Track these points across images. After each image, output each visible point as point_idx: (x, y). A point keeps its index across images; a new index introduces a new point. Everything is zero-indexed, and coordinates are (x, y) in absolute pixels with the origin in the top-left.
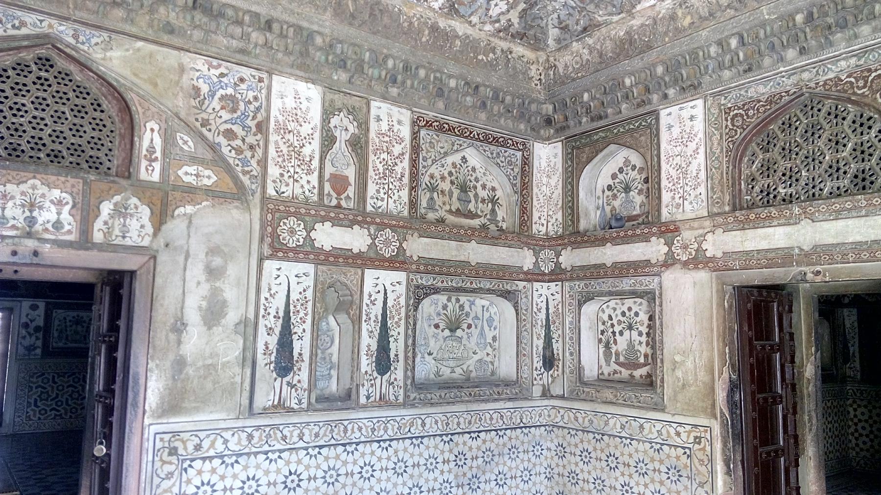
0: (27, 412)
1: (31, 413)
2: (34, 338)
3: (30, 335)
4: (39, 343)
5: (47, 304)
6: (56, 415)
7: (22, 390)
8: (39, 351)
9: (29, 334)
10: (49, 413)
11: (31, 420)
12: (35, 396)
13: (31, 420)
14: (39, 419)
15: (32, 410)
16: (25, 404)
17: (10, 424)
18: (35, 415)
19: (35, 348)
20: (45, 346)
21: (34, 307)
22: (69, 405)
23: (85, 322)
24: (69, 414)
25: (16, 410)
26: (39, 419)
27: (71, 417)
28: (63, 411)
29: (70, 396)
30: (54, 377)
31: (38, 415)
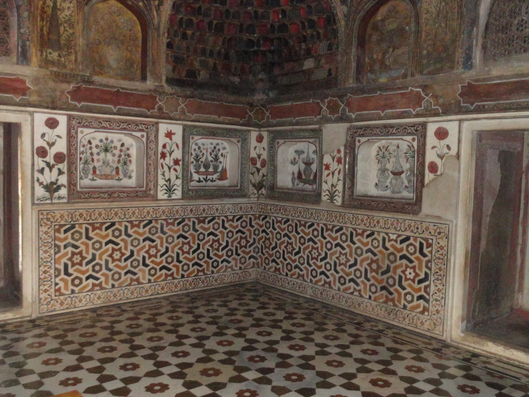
0: (56, 284)
1: (61, 284)
2: (55, 171)
3: (51, 167)
4: (63, 180)
5: (70, 118)
6: (94, 285)
7: (46, 252)
8: (63, 192)
9: (48, 164)
10: (85, 283)
11: (61, 294)
12: (64, 260)
13: (61, 294)
14: (73, 292)
15: (62, 280)
16: (52, 271)
17: (33, 302)
18: (66, 288)
19: (59, 188)
20: (71, 184)
21: (52, 124)
22: (110, 270)
23: (115, 148)
24: (111, 282)
25: (41, 281)
26: (73, 292)
27: (113, 286)
28: (103, 279)
29: (111, 256)
30: (87, 230)
31: (71, 287)
